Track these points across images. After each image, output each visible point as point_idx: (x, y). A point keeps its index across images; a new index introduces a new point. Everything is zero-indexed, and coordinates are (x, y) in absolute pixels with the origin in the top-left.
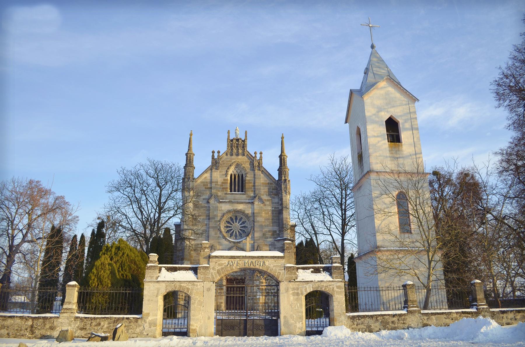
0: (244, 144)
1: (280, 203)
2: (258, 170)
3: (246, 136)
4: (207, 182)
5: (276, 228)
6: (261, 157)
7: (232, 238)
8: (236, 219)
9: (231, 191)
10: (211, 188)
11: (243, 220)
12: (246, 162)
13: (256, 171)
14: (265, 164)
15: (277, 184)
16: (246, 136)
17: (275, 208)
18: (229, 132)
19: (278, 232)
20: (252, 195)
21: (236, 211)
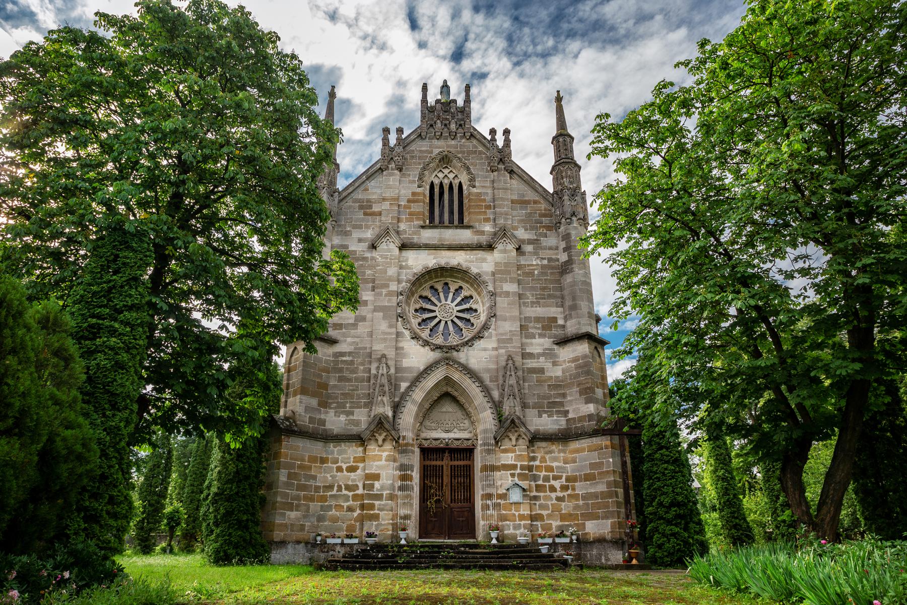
1: (563, 245)
5: (554, 311)
6: (507, 142)
11: (464, 293)
14: (516, 158)
17: (550, 260)
18: (425, 88)
19: (561, 322)
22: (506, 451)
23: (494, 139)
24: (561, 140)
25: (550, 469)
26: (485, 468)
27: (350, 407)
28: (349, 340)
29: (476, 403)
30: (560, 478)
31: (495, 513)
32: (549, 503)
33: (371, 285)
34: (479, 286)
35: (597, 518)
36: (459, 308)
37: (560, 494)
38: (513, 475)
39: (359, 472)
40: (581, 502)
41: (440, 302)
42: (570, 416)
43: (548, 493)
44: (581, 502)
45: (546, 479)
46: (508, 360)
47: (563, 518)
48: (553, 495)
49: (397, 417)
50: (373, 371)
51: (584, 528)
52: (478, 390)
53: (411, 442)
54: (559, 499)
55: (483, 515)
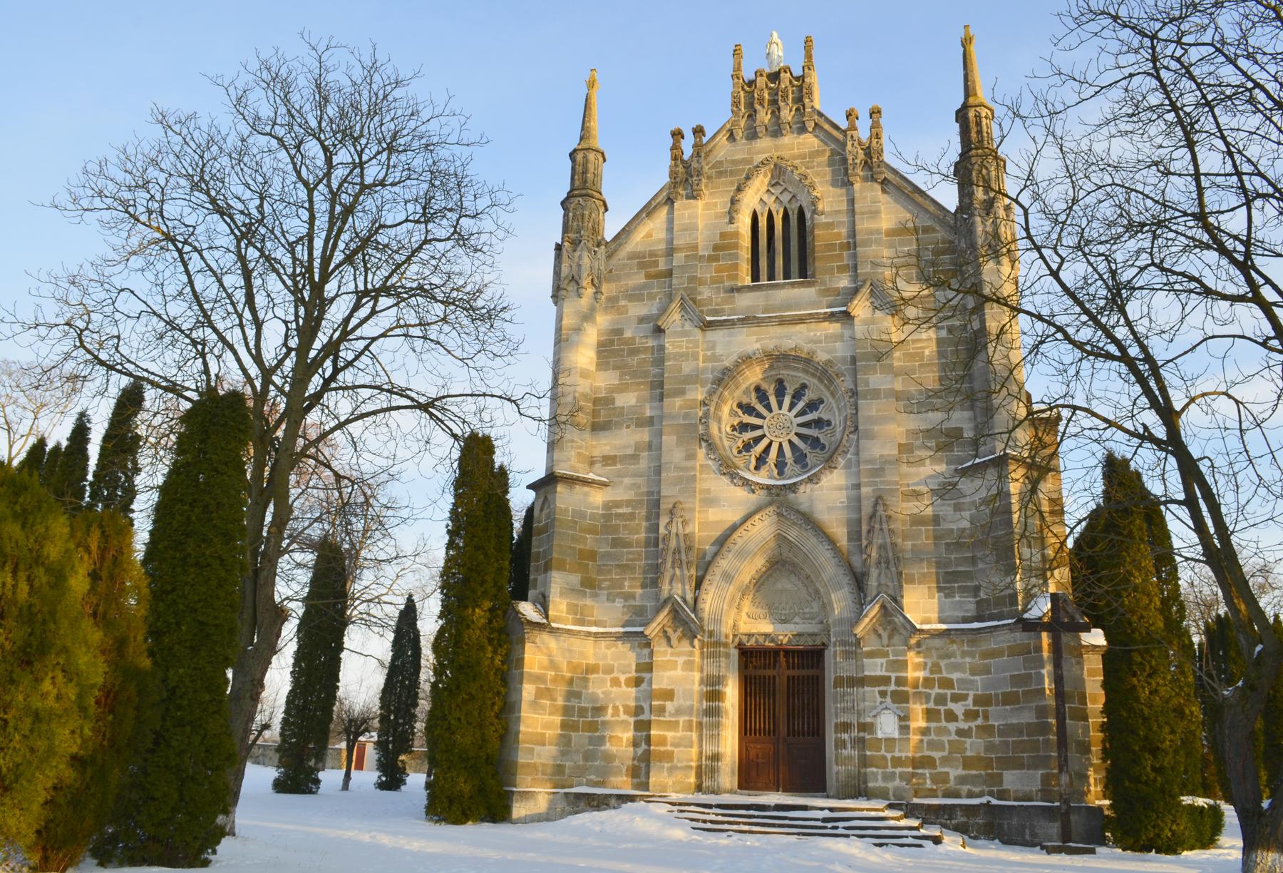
0: (800, 88)
2: (865, 179)
3: (809, 56)
4: (653, 254)
7: (764, 470)
8: (780, 393)
9: (755, 276)
10: (669, 274)
11: (809, 395)
12: (814, 154)
13: (857, 186)
15: (954, 229)
16: (809, 56)
18: (737, 52)
20: (844, 282)
21: (778, 358)
22: (871, 655)
23: (853, 128)
24: (971, 114)
25: (947, 683)
26: (839, 682)
27: (630, 587)
28: (627, 481)
29: (825, 576)
30: (964, 698)
31: (854, 753)
32: (945, 739)
33: (658, 391)
34: (831, 381)
35: (1021, 766)
36: (801, 420)
37: (964, 726)
38: (883, 694)
39: (644, 686)
40: (997, 740)
41: (771, 411)
42: (983, 595)
43: (944, 723)
44: (997, 740)
45: (941, 700)
46: (876, 504)
47: (967, 763)
48: (952, 727)
49: (700, 601)
50: (662, 530)
51: (1001, 782)
52: (829, 554)
53: (723, 640)
54: (960, 733)
55: (837, 756)
